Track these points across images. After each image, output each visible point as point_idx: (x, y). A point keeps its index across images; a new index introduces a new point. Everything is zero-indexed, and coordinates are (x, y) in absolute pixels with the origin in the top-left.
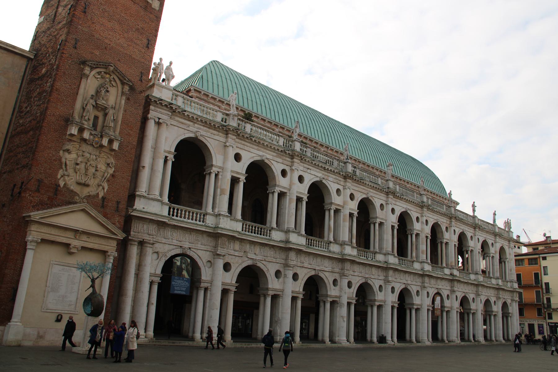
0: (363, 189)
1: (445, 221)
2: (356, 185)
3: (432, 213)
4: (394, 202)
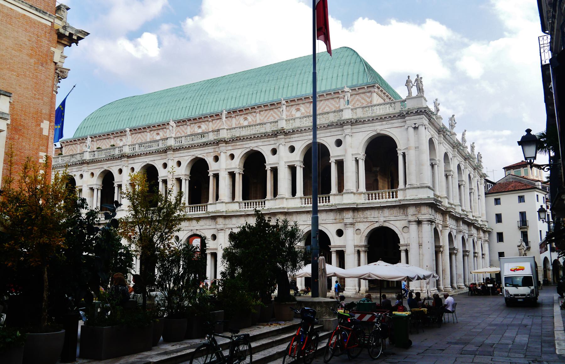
0: (101, 165)
1: (212, 150)
2: (94, 164)
3: (185, 151)
4: (132, 162)
